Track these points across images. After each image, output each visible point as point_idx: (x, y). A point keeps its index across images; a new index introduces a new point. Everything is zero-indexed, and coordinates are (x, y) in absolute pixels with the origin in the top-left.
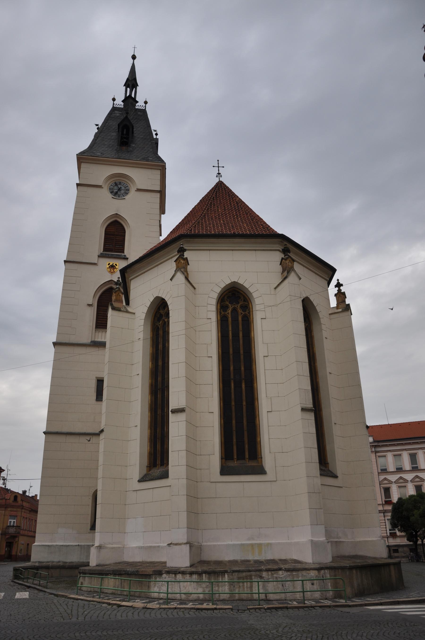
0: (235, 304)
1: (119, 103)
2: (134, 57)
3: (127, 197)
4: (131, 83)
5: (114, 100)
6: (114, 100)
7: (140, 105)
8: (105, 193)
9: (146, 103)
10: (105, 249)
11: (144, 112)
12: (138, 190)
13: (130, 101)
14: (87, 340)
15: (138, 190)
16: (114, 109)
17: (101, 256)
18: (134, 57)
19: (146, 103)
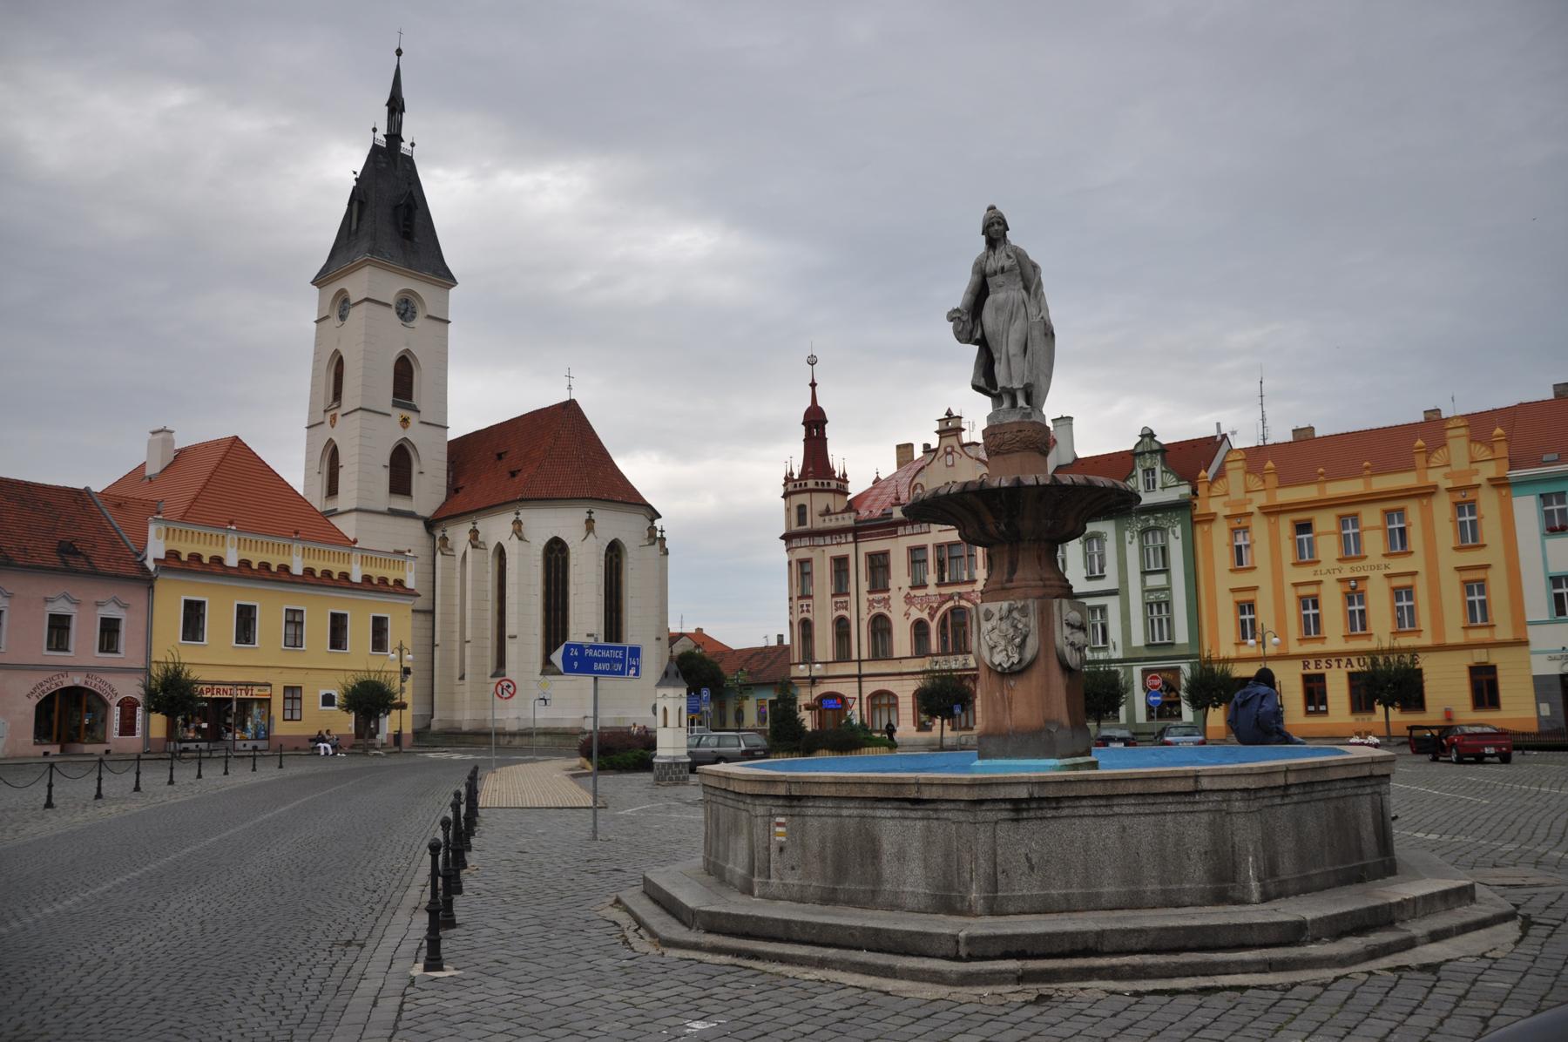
0: (614, 552)
1: (382, 141)
2: (399, 53)
3: (415, 323)
4: (396, 106)
5: (375, 130)
6: (375, 130)
7: (405, 147)
8: (393, 313)
9: (413, 145)
10: (395, 395)
11: (409, 161)
12: (429, 317)
13: (394, 137)
14: (384, 508)
15: (429, 317)
16: (375, 149)
17: (395, 405)
18: (399, 53)
19: (413, 145)
